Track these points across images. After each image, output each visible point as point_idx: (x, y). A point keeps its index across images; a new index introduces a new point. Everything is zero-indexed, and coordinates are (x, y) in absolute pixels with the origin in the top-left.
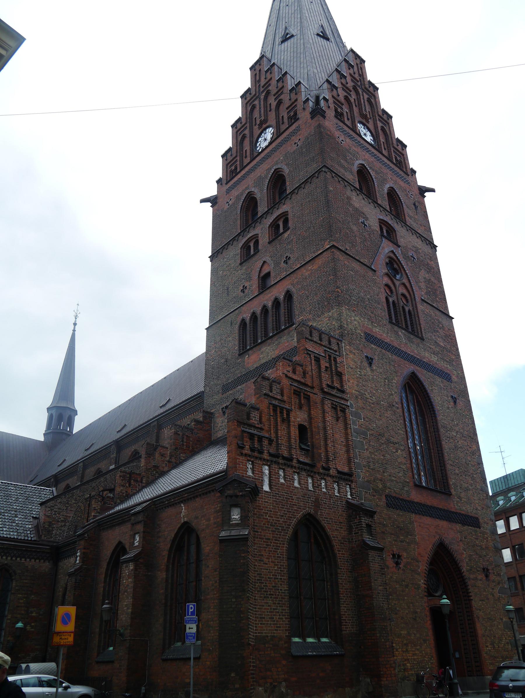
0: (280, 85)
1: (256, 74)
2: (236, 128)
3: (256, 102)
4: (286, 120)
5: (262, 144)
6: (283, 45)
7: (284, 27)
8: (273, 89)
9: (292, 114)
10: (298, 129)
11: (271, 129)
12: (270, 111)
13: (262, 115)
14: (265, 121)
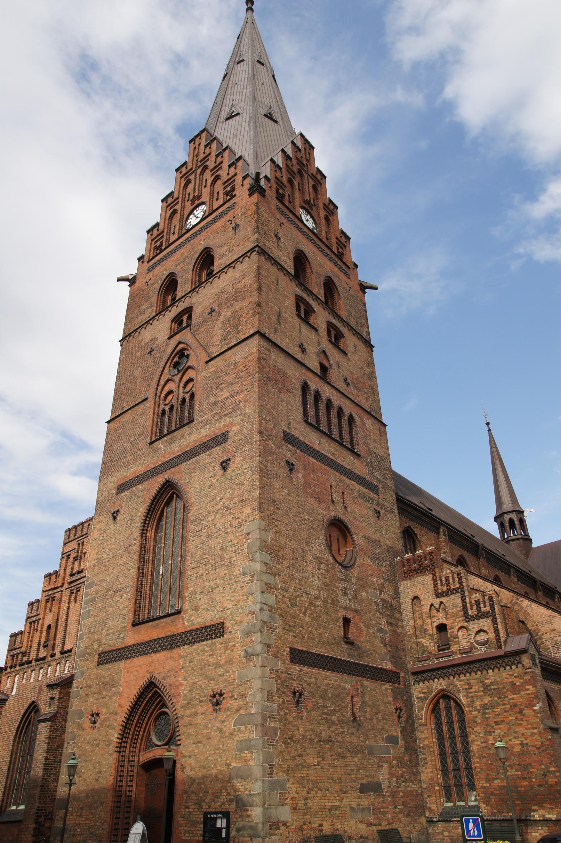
0: (219, 160)
1: (195, 148)
2: (167, 202)
3: (192, 177)
4: (221, 195)
5: (193, 221)
6: (227, 122)
7: (230, 104)
8: (211, 164)
9: (229, 189)
10: (232, 207)
11: (204, 206)
12: (205, 186)
13: (197, 190)
14: (199, 197)
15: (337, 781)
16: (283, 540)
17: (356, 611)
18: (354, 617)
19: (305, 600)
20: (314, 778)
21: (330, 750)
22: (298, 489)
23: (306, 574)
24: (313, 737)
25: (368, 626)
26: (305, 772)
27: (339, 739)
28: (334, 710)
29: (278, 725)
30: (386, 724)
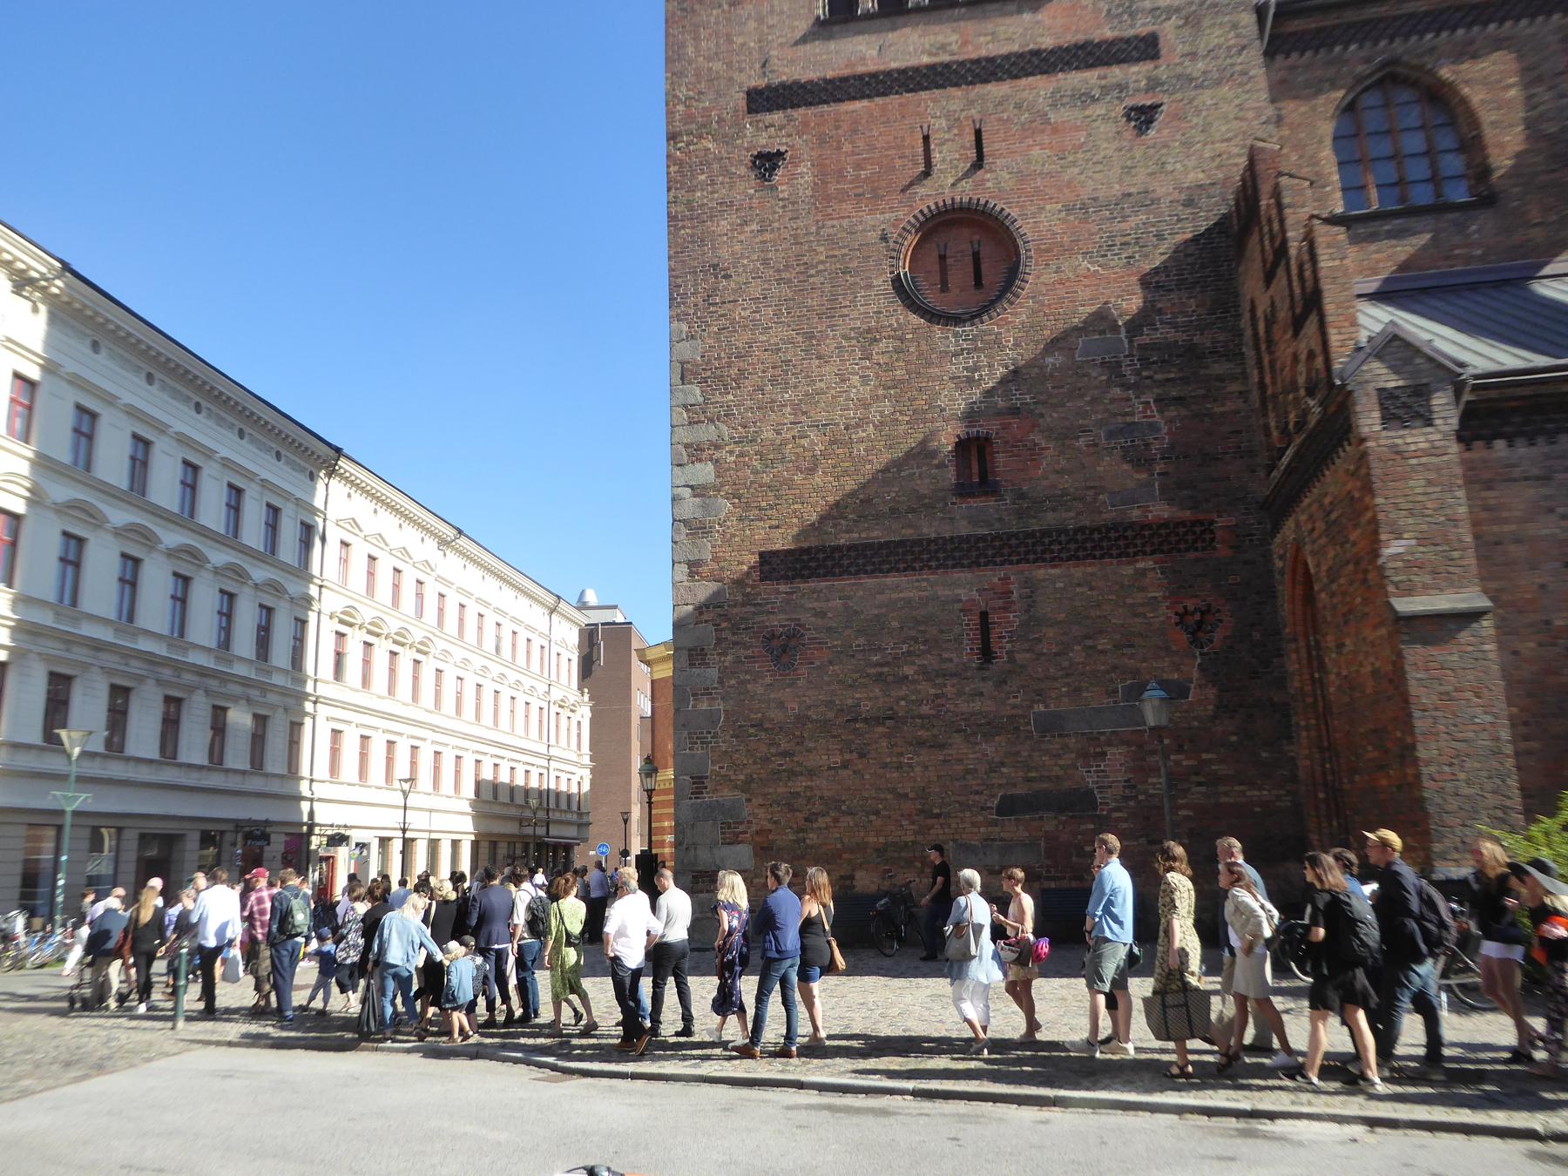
15: (911, 795)
16: (740, 340)
17: (1014, 411)
18: (1005, 427)
19: (812, 443)
20: (826, 794)
21: (887, 736)
22: (793, 203)
23: (819, 385)
24: (831, 715)
25: (1064, 436)
26: (800, 784)
27: (925, 709)
28: (909, 653)
29: (720, 706)
30: (1132, 656)
